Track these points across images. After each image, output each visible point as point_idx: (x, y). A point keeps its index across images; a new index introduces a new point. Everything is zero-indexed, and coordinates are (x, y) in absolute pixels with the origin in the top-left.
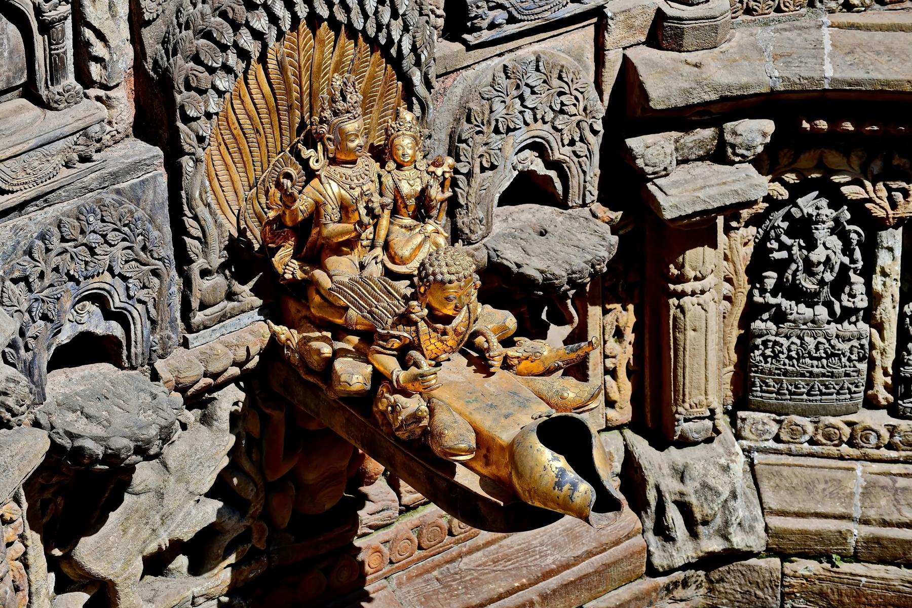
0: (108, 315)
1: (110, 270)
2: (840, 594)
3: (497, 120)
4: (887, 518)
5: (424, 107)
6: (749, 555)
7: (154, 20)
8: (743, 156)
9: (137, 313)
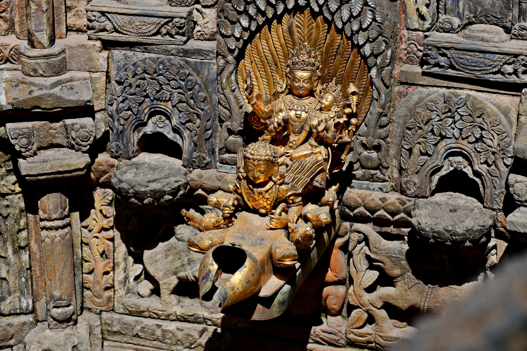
3: (433, 126)
5: (379, 94)
9: (186, 134)
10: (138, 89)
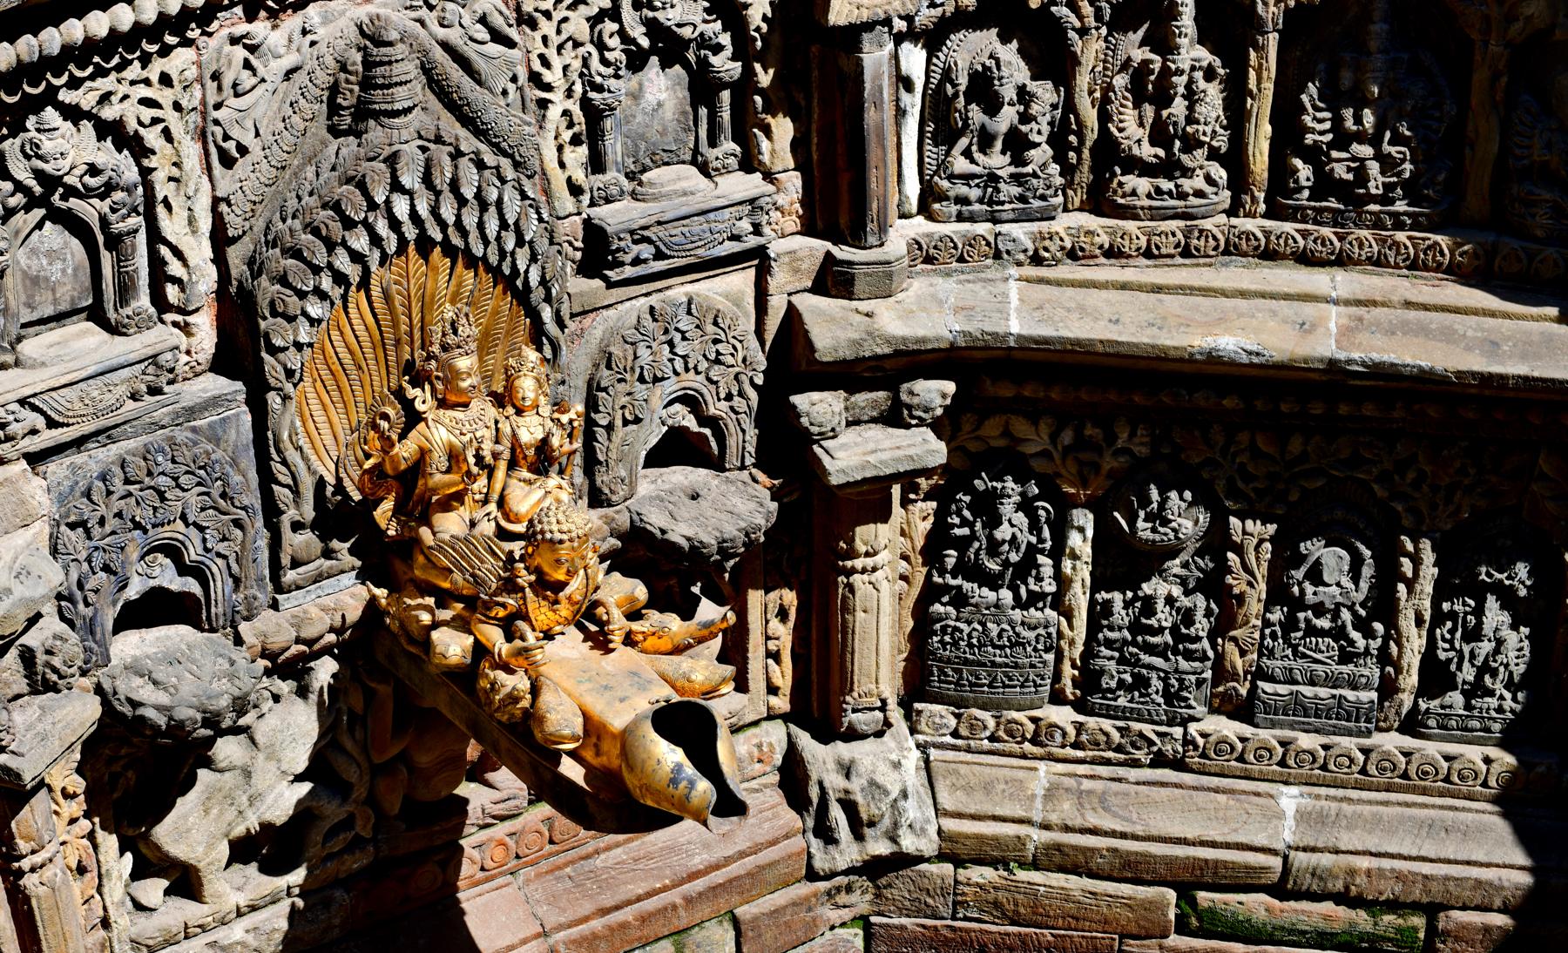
0: (183, 569)
1: (184, 517)
2: (1016, 905)
4: (1070, 823)
5: (556, 349)
6: (920, 859)
7: (240, 237)
8: (919, 418)
9: (216, 567)
10: (117, 521)
